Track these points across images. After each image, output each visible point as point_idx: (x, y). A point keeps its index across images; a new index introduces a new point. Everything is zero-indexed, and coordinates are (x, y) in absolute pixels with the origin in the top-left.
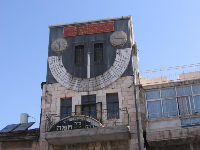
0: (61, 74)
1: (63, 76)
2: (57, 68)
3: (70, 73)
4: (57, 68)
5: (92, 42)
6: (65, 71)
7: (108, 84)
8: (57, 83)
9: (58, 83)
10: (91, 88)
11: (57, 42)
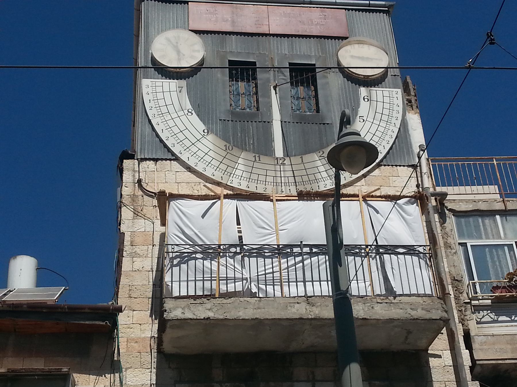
0: (186, 132)
1: (194, 140)
2: (174, 115)
3: (216, 135)
4: (174, 115)
6: (201, 126)
8: (172, 161)
10: (288, 188)
11: (168, 40)
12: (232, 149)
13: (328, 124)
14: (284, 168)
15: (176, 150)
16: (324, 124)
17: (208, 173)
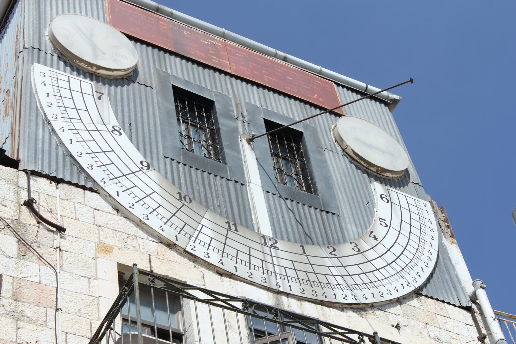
4: (90, 127)
5: (253, 110)
7: (370, 300)
8: (87, 192)
9: (94, 189)
12: (190, 202)
13: (333, 214)
14: (276, 253)
15: (97, 174)
16: (327, 212)
17: (154, 223)
